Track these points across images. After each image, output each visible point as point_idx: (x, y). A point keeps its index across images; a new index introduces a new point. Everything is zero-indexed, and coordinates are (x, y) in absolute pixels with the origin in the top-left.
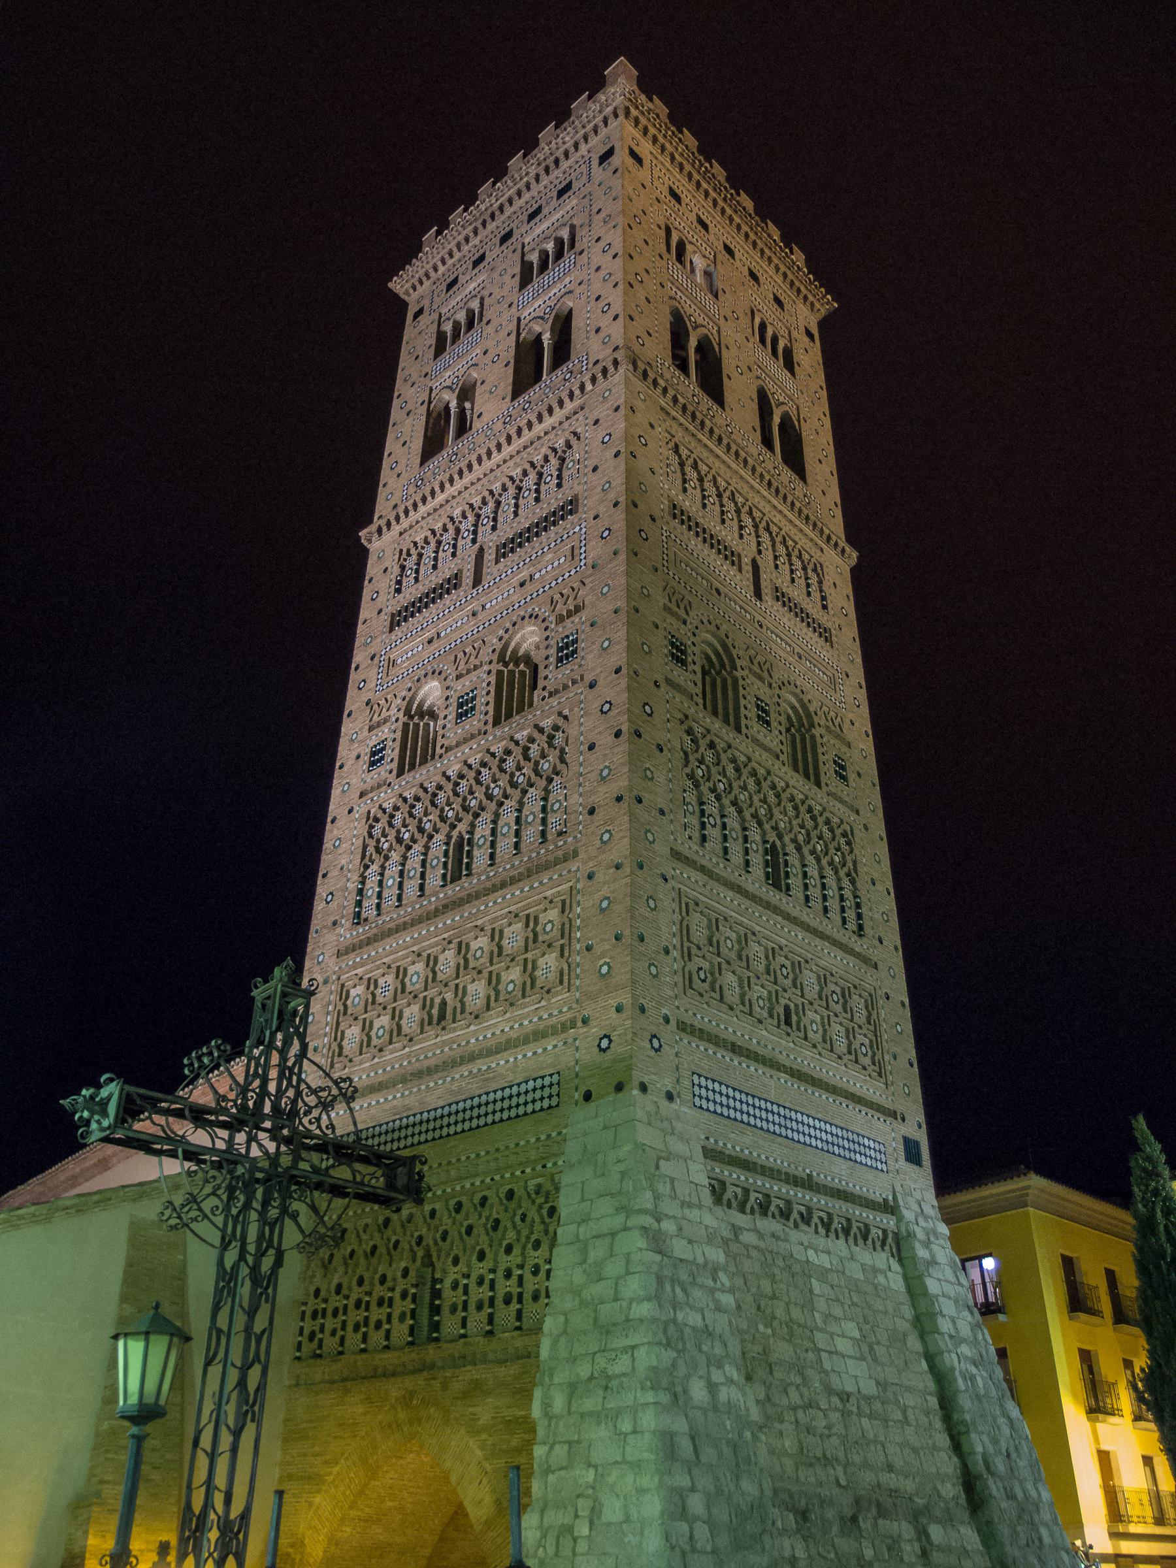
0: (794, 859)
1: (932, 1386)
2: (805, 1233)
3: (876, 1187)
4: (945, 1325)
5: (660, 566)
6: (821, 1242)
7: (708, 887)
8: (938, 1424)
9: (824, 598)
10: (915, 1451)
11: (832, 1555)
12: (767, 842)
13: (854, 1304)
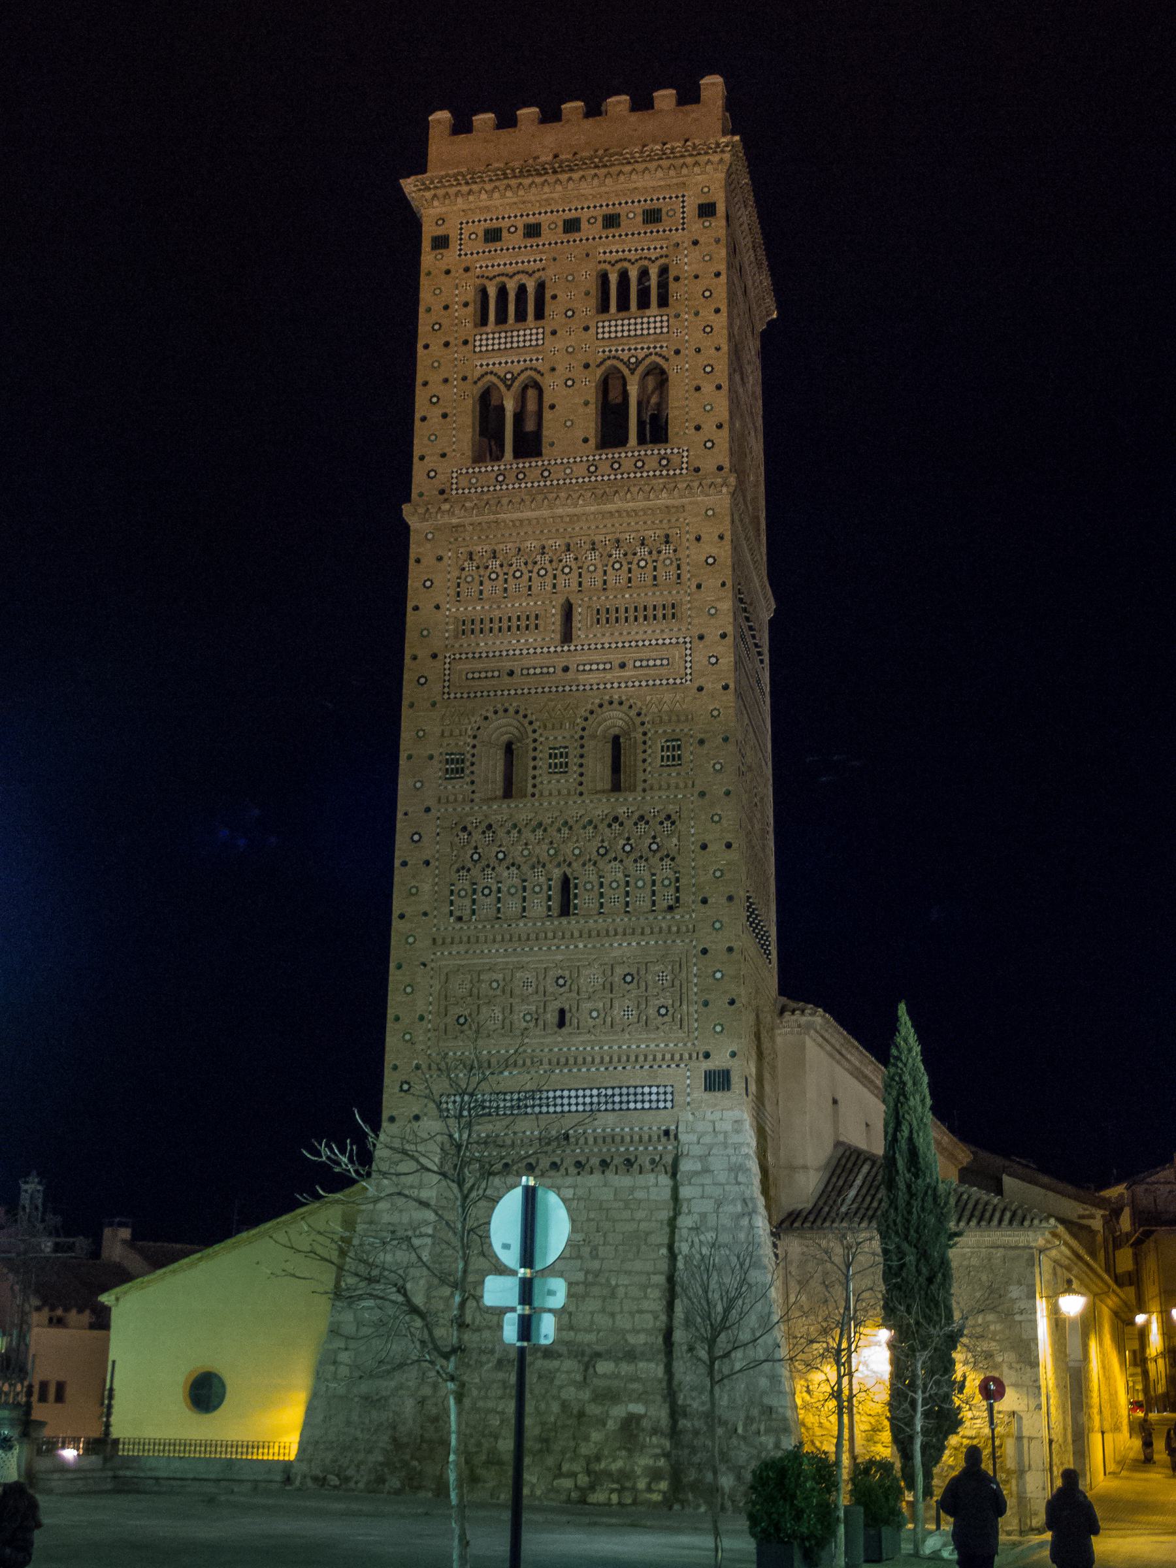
0: (586, 877)
1: (664, 1266)
2: (550, 1177)
3: (655, 1123)
4: (685, 1222)
5: (438, 698)
6: (569, 1180)
7: (471, 952)
8: (655, 1294)
9: (679, 567)
10: (613, 1315)
11: (477, 1380)
12: (550, 880)
13: (589, 1220)
